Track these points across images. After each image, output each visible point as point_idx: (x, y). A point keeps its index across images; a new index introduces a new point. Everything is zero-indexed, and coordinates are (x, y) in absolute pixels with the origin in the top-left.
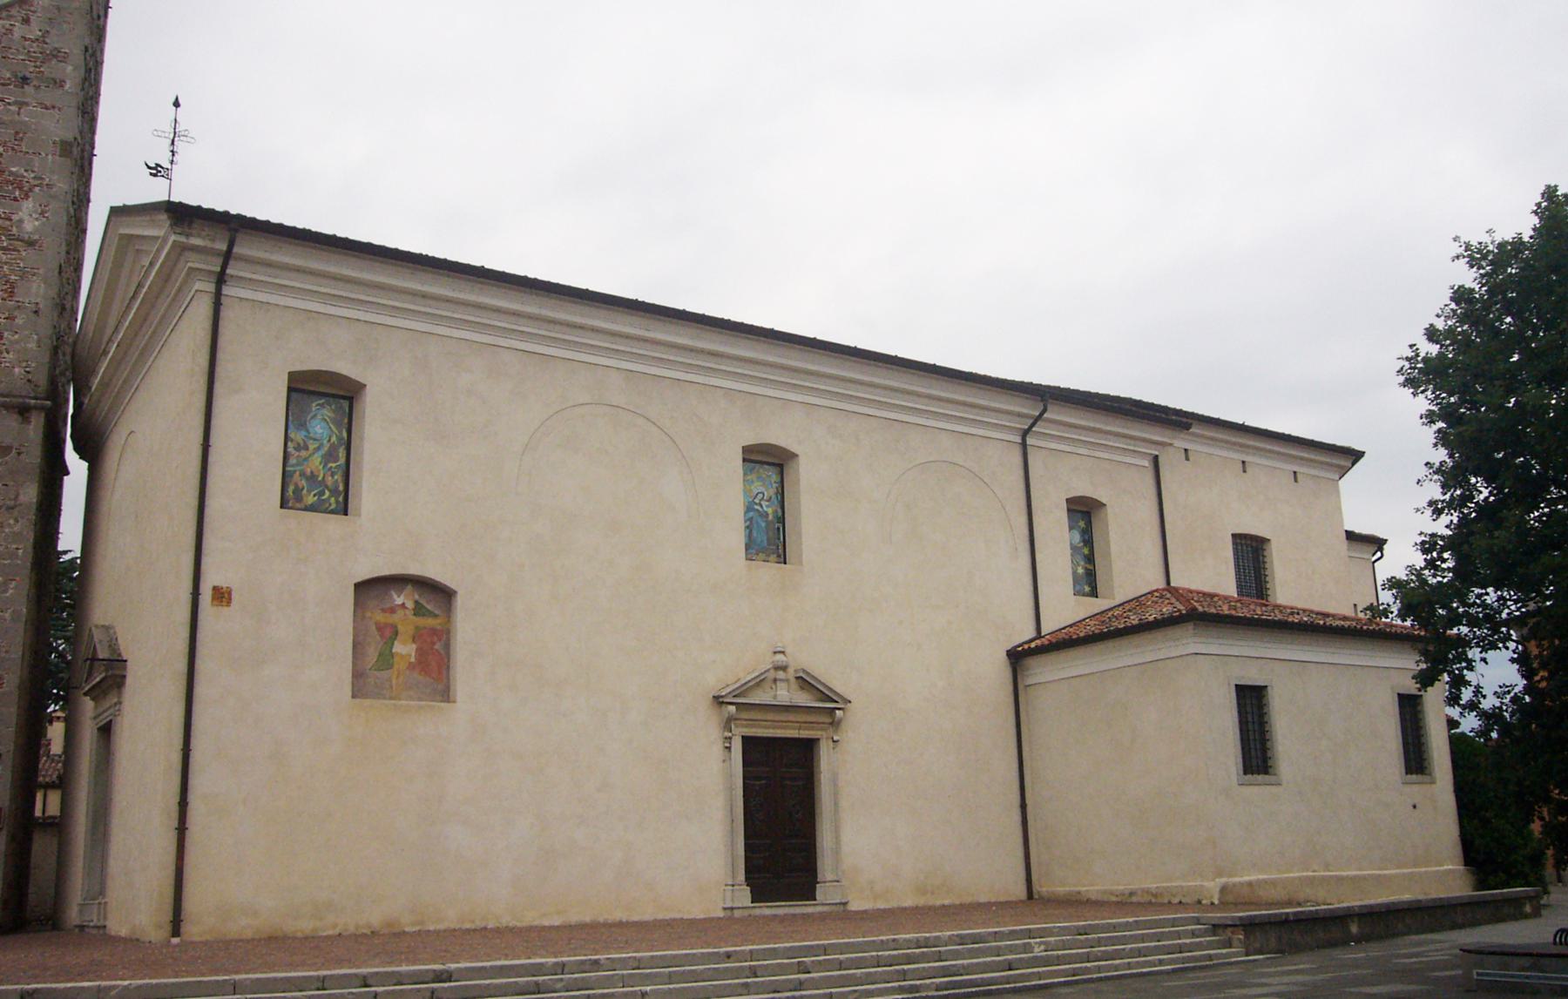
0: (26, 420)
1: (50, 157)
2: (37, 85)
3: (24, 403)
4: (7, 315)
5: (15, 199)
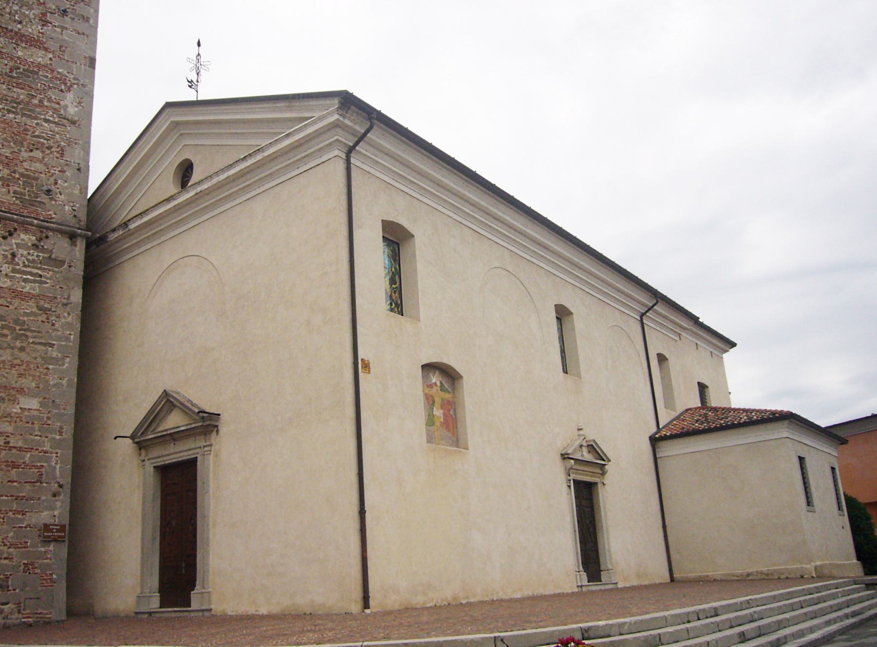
0: (74, 244)
1: (83, 66)
2: (72, 16)
3: (74, 231)
4: (60, 169)
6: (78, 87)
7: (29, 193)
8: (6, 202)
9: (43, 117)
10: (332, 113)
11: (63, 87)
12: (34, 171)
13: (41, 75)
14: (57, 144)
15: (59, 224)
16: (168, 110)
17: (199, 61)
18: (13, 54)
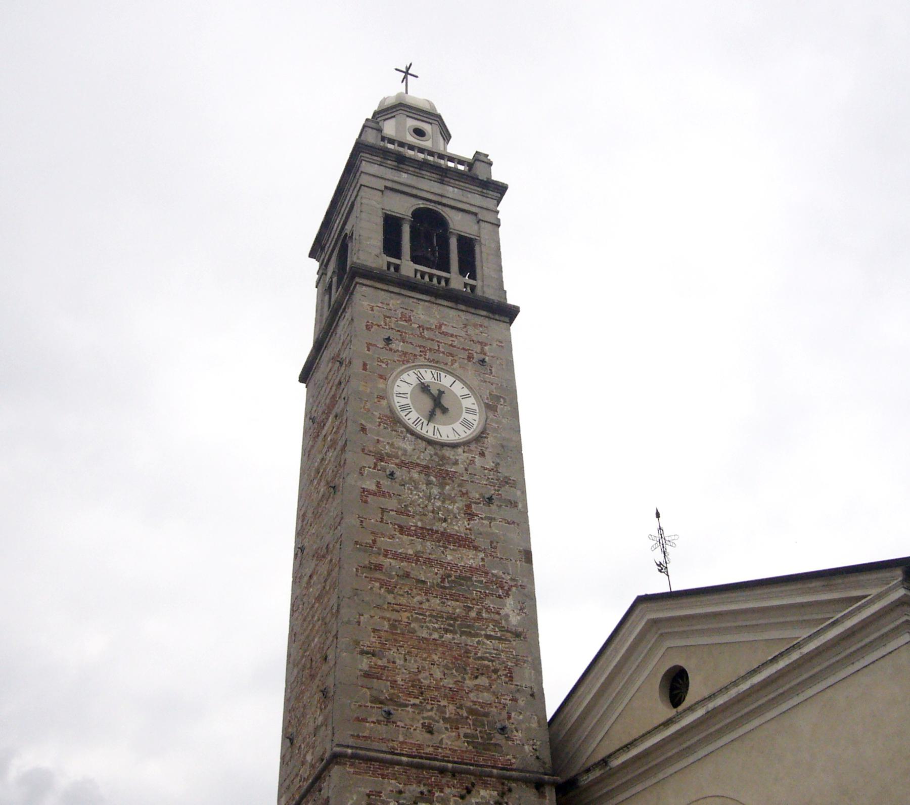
0: (542, 795)
1: (518, 562)
2: (499, 504)
5: (500, 597)
6: (516, 590)
7: (482, 735)
8: (457, 750)
9: (483, 633)
10: (895, 588)
11: (501, 592)
12: (483, 703)
13: (476, 581)
14: (504, 665)
15: (521, 771)
16: (641, 607)
17: (663, 536)
18: (442, 560)
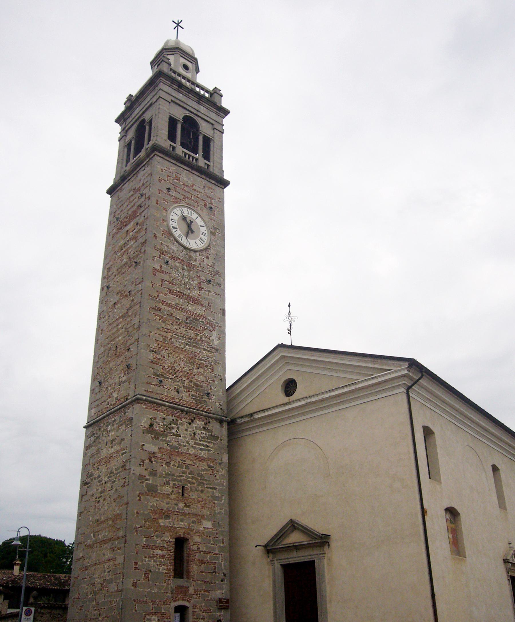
0: (222, 426)
1: (219, 315)
2: (213, 284)
3: (222, 418)
4: (212, 379)
5: (210, 331)
9: (202, 347)
11: (211, 328)
13: (201, 322)
15: (214, 414)
16: (279, 349)
